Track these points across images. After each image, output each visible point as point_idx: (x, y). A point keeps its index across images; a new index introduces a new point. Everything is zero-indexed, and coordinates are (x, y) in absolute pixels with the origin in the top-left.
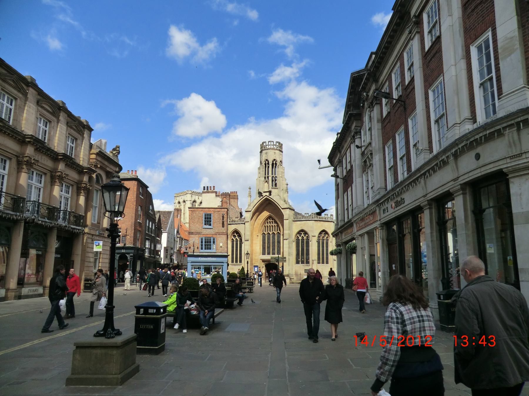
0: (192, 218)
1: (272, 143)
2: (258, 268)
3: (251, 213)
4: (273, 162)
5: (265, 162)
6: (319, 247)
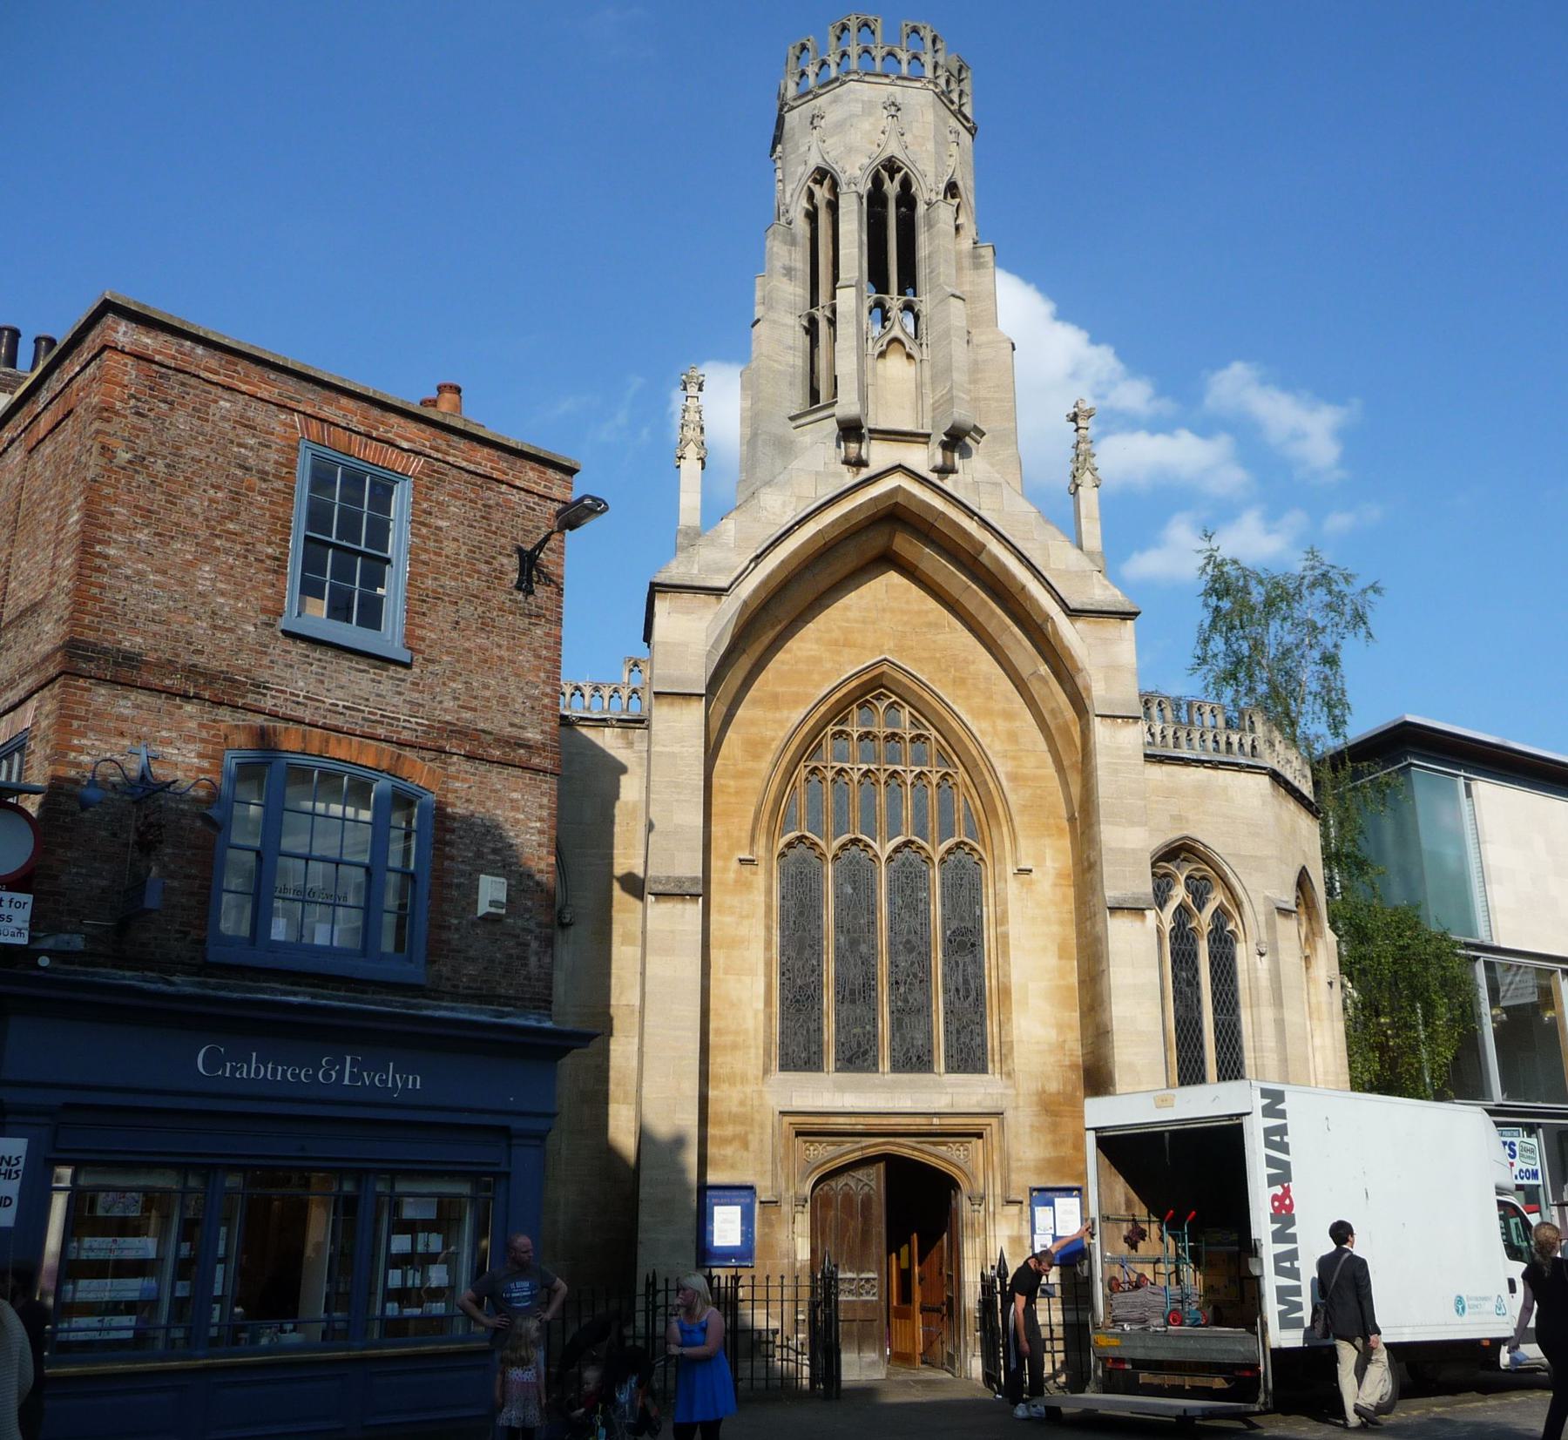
2: (747, 1219)
3: (730, 607)
5: (811, 196)
6: (1227, 1002)
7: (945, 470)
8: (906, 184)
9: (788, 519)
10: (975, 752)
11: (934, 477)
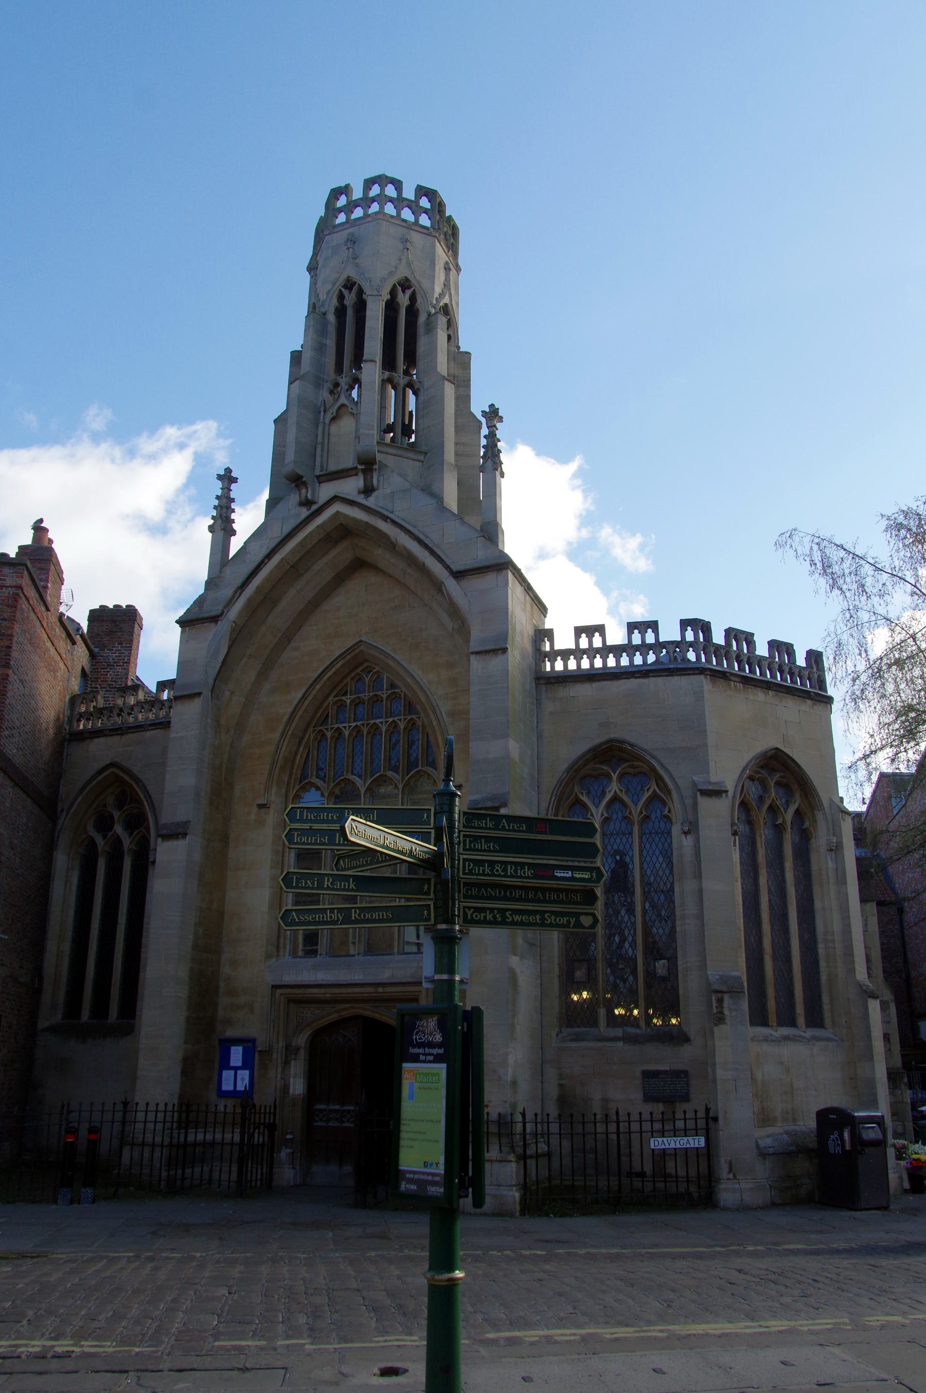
1: (390, 191)
3: (224, 626)
4: (393, 292)
7: (368, 490)
8: (361, 291)
10: (423, 699)
11: (361, 499)
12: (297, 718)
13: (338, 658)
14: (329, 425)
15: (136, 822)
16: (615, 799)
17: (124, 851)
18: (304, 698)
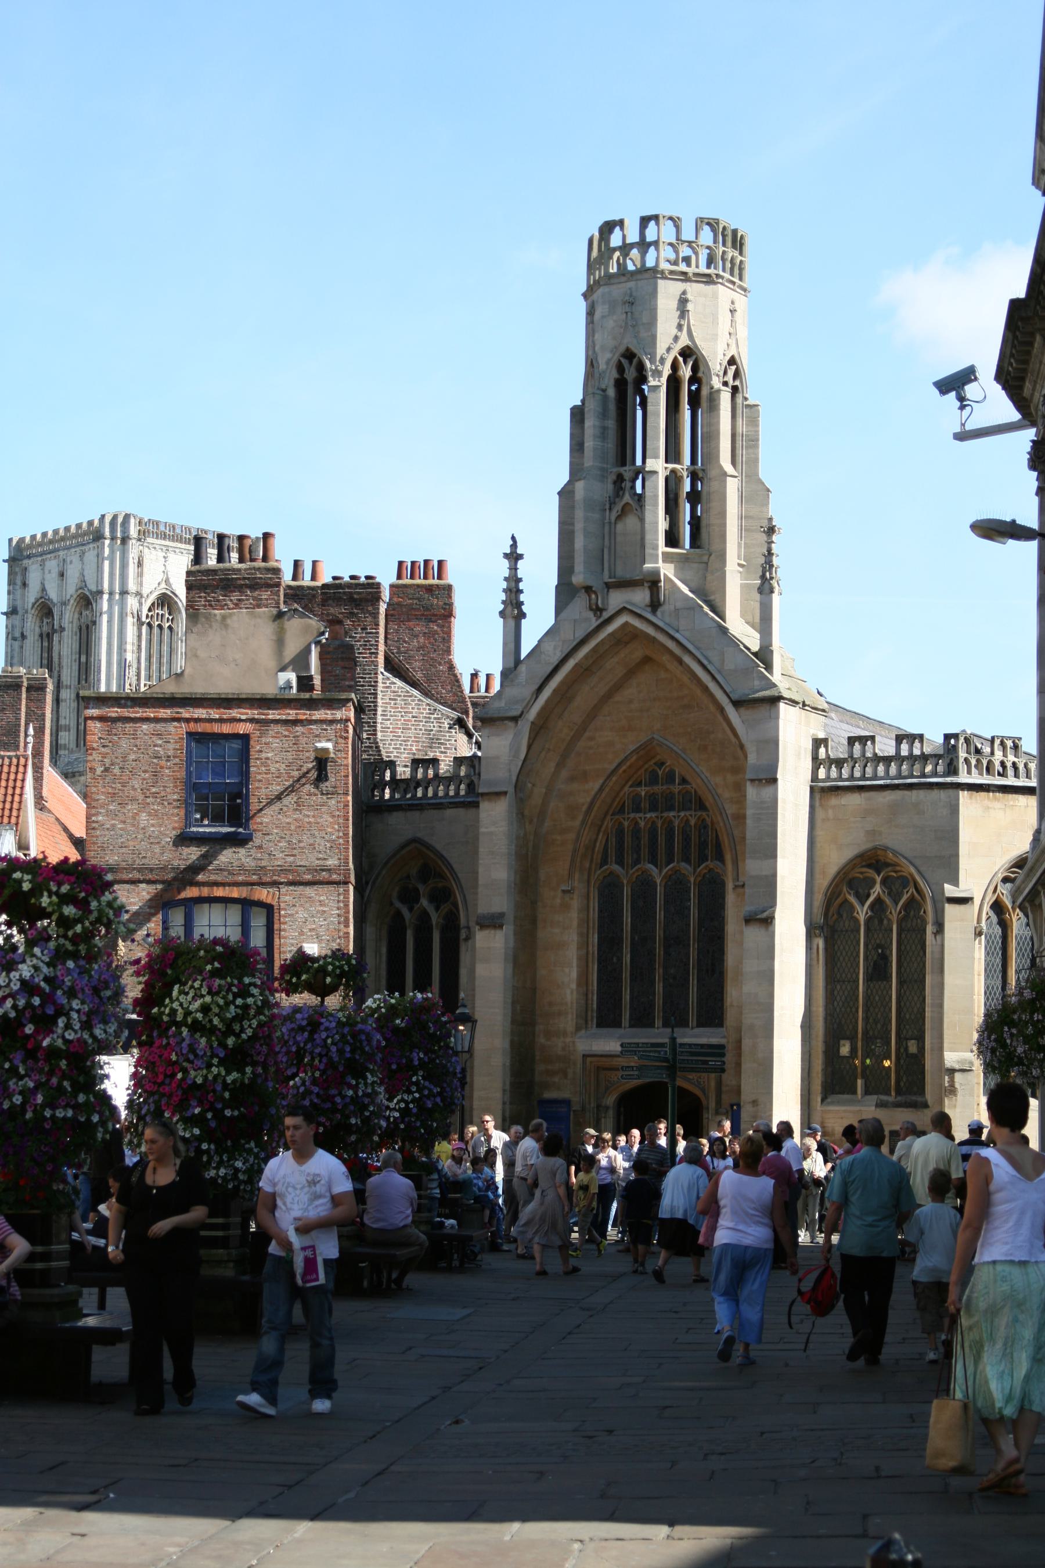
0: (106, 770)
1: (668, 232)
3: (524, 728)
4: (675, 366)
9: (555, 660)
12: (596, 808)
13: (632, 752)
14: (615, 523)
15: (443, 896)
16: (878, 900)
17: (432, 925)
18: (601, 789)
